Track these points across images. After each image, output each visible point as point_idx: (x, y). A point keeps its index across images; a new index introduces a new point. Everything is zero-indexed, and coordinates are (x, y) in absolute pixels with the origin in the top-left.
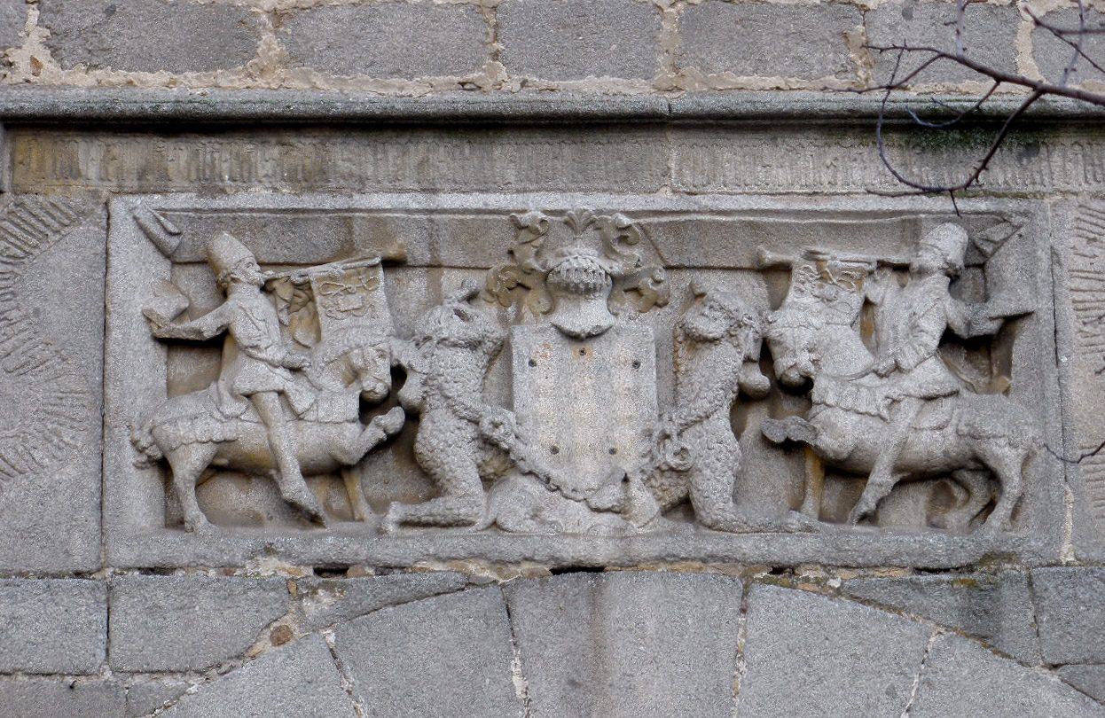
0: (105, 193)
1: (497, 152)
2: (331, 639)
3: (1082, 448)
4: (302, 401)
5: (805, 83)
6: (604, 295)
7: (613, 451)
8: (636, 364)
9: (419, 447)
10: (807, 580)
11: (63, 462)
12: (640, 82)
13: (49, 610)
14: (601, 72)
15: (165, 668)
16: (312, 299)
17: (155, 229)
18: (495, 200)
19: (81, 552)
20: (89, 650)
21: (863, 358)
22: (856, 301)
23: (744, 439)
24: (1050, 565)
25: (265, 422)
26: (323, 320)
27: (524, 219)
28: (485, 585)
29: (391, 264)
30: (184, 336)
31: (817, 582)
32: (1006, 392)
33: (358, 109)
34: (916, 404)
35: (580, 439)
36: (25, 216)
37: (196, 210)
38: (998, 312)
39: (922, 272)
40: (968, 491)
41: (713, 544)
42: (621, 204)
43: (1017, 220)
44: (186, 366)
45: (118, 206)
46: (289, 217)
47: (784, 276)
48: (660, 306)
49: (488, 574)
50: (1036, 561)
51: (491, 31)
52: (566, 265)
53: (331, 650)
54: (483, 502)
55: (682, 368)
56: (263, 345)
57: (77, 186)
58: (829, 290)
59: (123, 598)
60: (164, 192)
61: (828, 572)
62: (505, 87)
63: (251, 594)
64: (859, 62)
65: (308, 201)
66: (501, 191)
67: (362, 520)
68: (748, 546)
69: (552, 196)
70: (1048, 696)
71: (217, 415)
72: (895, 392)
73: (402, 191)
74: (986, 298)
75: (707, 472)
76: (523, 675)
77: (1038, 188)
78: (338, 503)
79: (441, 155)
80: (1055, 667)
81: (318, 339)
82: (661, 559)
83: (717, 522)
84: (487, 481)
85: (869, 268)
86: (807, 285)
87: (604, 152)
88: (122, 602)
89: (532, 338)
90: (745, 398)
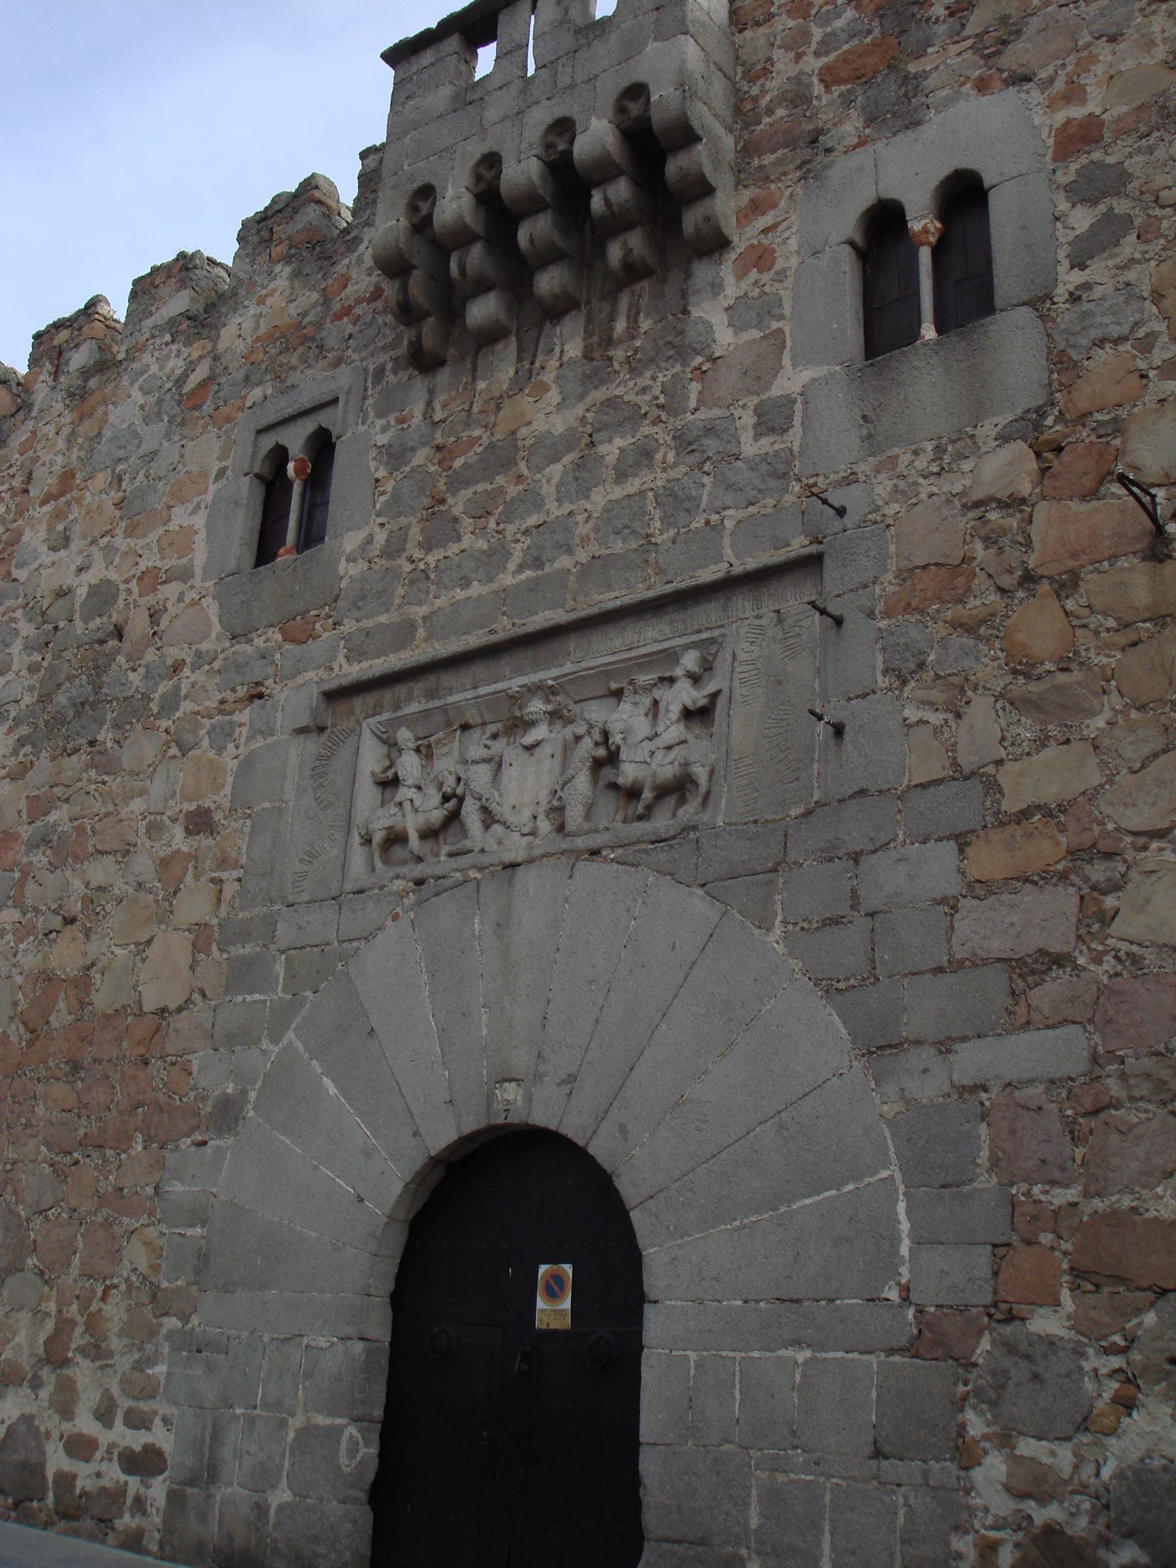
1: (503, 662)
12: (560, 611)
14: (544, 609)
17: (377, 732)
18: (500, 686)
22: (647, 701)
25: (404, 816)
41: (564, 846)
42: (547, 675)
57: (352, 718)
65: (431, 705)
79: (480, 670)
80: (703, 885)
84: (487, 826)
88: (344, 909)
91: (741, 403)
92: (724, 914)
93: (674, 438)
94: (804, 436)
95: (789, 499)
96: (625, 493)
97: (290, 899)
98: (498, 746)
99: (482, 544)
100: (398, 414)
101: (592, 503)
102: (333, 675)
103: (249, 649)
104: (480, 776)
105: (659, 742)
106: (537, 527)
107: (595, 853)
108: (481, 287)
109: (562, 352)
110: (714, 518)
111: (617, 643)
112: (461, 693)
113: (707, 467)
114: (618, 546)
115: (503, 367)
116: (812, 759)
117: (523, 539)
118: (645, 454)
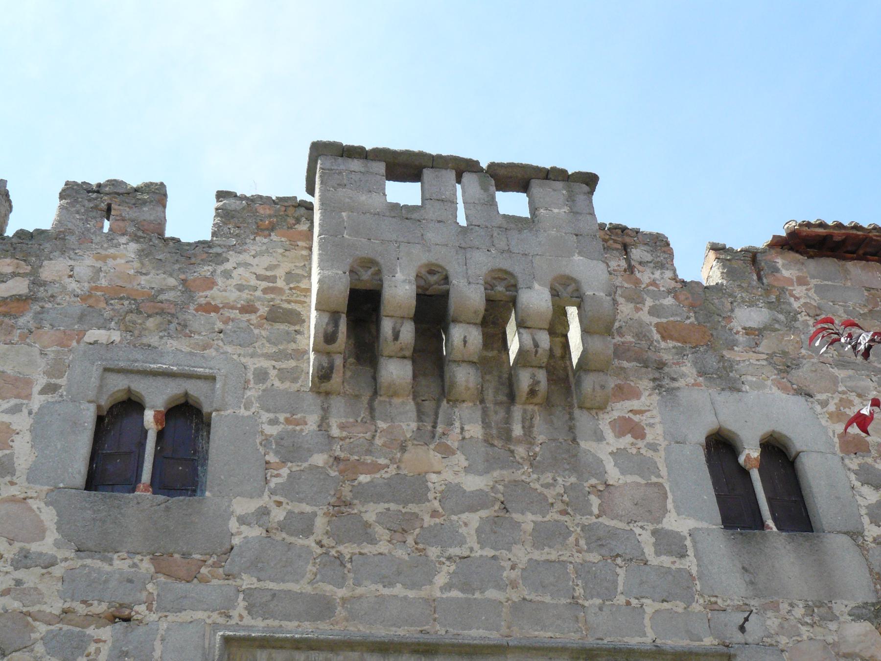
5: (562, 636)
62: (439, 633)
91: (640, 524)
93: (582, 530)
94: (699, 566)
95: (696, 607)
96: (544, 557)
99: (400, 553)
100: (288, 415)
101: (515, 555)
102: (233, 622)
103: (106, 567)
106: (461, 558)
109: (462, 429)
110: (634, 602)
113: (619, 561)
114: (548, 599)
117: (448, 563)
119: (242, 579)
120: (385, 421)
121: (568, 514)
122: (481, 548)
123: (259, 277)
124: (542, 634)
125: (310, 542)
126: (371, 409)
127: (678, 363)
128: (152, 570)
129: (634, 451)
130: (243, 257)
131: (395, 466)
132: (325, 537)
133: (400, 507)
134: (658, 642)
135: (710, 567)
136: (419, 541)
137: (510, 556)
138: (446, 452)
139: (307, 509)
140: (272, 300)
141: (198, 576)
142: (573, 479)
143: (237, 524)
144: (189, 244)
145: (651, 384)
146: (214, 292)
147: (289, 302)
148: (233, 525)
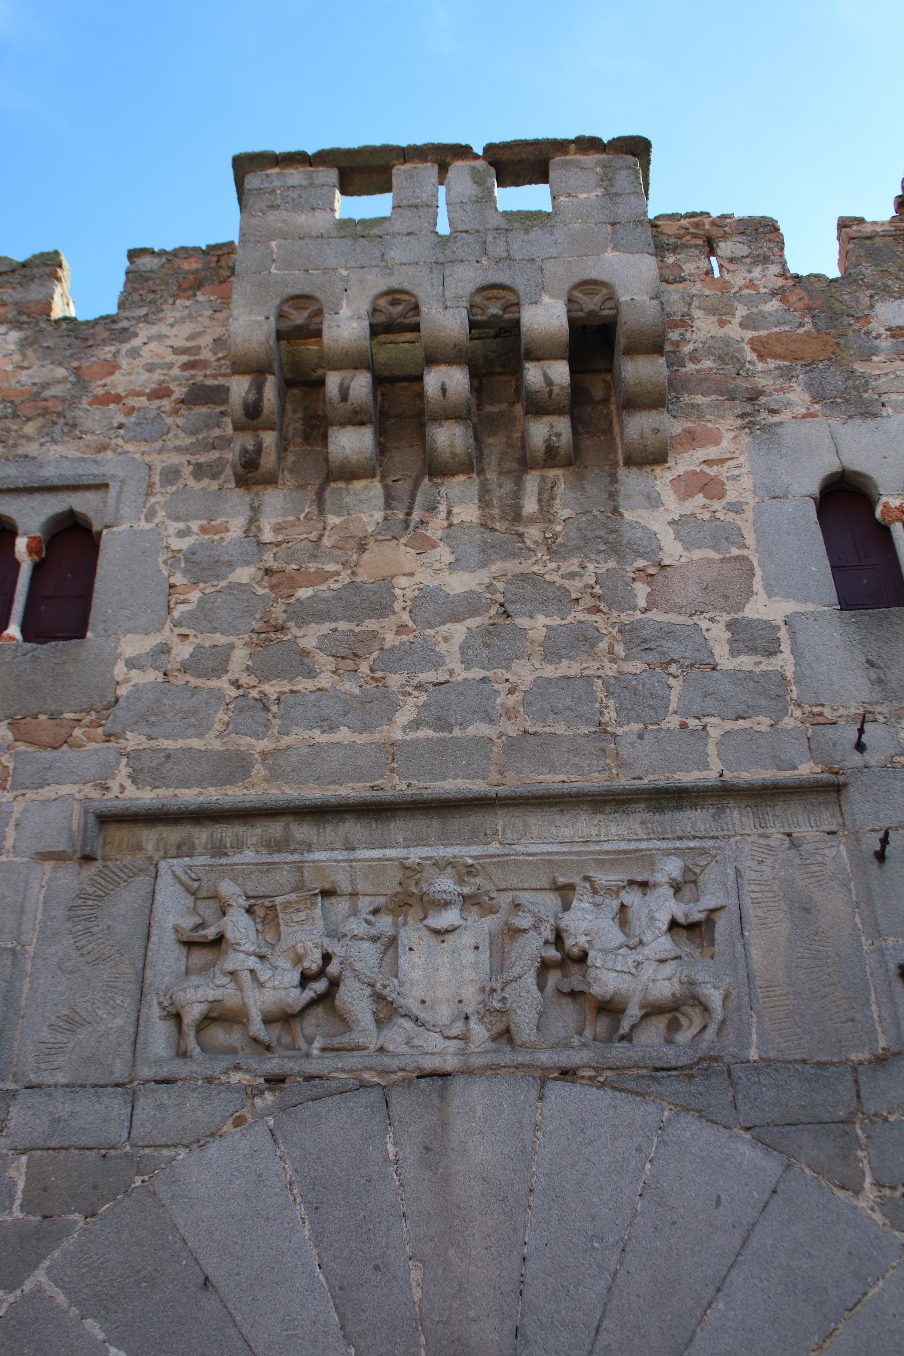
0: (156, 858)
2: (271, 1122)
3: (761, 988)
4: (264, 974)
5: (580, 778)
6: (459, 906)
7: (460, 1002)
8: (477, 948)
9: (337, 1003)
10: (583, 1077)
11: (115, 1016)
13: (96, 1107)
14: (456, 777)
15: (164, 1143)
16: (277, 916)
17: (184, 878)
19: (120, 1072)
20: (116, 1132)
21: (620, 938)
22: (615, 904)
23: (546, 993)
24: (743, 1063)
25: (241, 989)
26: (283, 928)
27: (408, 863)
28: (374, 1086)
29: (327, 894)
30: (197, 940)
31: (590, 1078)
32: (712, 957)
33: (307, 802)
34: (654, 965)
35: (440, 995)
36: (108, 872)
37: (210, 865)
38: (705, 907)
39: (655, 885)
40: (691, 1020)
42: (468, 852)
43: (713, 852)
44: (199, 957)
45: (163, 865)
46: (265, 867)
47: (571, 892)
48: (494, 913)
49: (376, 1079)
50: (734, 1061)
51: (390, 757)
52: (433, 889)
53: (271, 1130)
54: (376, 1034)
55: (507, 950)
56: (242, 942)
57: (140, 855)
58: (598, 899)
59: (142, 1100)
60: (191, 856)
61: (597, 1072)
62: (398, 788)
63: (222, 1095)
64: (612, 765)
66: (394, 847)
67: (299, 1049)
68: (544, 1058)
69: (425, 849)
70: (746, 1149)
71: (211, 985)
72: (640, 958)
73: (332, 850)
74: (698, 900)
75: (519, 1011)
76: (395, 1144)
77: (726, 832)
78: (286, 1039)
80: (748, 1129)
81: (279, 940)
82: (488, 1067)
83: (525, 1043)
84: (380, 1023)
85: (622, 884)
86: (585, 896)
87: (458, 823)
88: (141, 1102)
89: (411, 934)
90: (545, 966)
91: (708, 615)
92: (788, 1166)
93: (620, 631)
94: (797, 664)
95: (788, 722)
96: (560, 673)
97: (33, 1078)
98: (385, 923)
99: (349, 686)
100: (204, 522)
101: (515, 674)
102: (111, 795)
104: (366, 955)
105: (646, 951)
106: (435, 685)
107: (567, 1074)
108: (356, 419)
109: (449, 513)
110: (692, 723)
111: (566, 832)
112: (328, 853)
113: (673, 669)
114: (561, 729)
115: (365, 506)
116: (868, 1001)
117: (416, 693)
118: (584, 641)
119: (127, 740)
120: (338, 514)
121: (600, 611)
122: (467, 669)
123: (176, 351)
124: (550, 777)
125: (223, 683)
126: (320, 500)
127: (782, 390)
128: (10, 736)
129: (706, 516)
130: (154, 330)
131: (349, 572)
132: (245, 674)
133: (353, 626)
134: (728, 775)
135: (814, 665)
136: (375, 667)
137: (508, 676)
138: (424, 545)
139: (220, 639)
140: (193, 377)
141: (70, 740)
142: (612, 564)
143: (125, 670)
144: (87, 323)
145: (739, 422)
146: (117, 377)
147: (215, 377)
148: (120, 670)
